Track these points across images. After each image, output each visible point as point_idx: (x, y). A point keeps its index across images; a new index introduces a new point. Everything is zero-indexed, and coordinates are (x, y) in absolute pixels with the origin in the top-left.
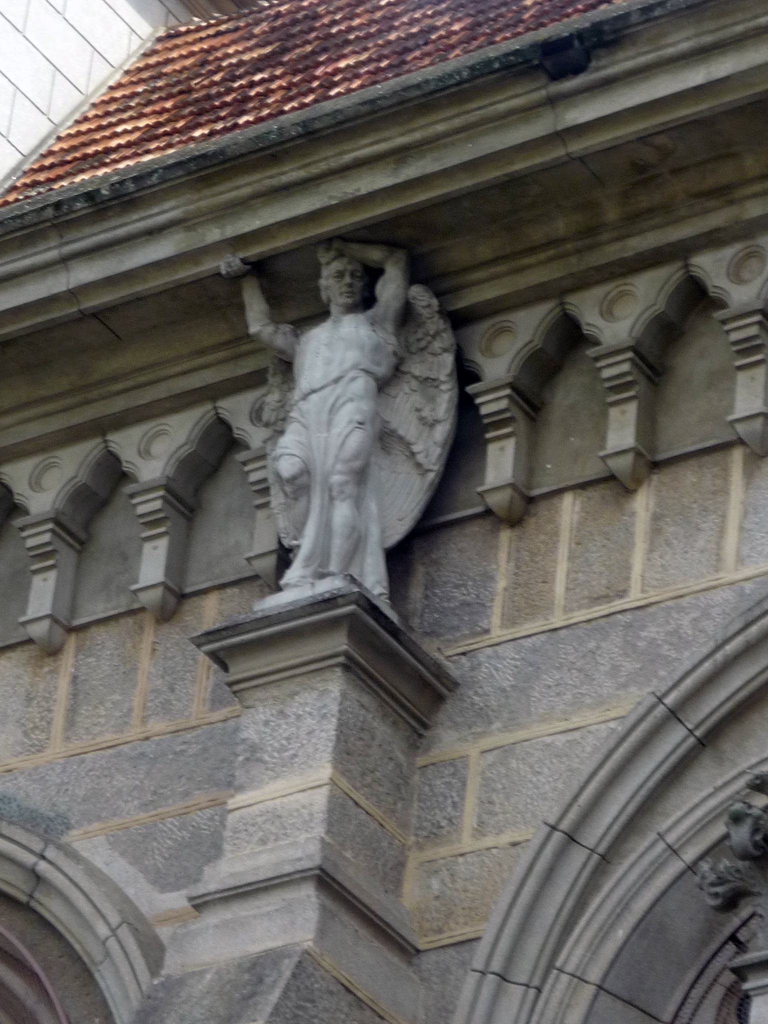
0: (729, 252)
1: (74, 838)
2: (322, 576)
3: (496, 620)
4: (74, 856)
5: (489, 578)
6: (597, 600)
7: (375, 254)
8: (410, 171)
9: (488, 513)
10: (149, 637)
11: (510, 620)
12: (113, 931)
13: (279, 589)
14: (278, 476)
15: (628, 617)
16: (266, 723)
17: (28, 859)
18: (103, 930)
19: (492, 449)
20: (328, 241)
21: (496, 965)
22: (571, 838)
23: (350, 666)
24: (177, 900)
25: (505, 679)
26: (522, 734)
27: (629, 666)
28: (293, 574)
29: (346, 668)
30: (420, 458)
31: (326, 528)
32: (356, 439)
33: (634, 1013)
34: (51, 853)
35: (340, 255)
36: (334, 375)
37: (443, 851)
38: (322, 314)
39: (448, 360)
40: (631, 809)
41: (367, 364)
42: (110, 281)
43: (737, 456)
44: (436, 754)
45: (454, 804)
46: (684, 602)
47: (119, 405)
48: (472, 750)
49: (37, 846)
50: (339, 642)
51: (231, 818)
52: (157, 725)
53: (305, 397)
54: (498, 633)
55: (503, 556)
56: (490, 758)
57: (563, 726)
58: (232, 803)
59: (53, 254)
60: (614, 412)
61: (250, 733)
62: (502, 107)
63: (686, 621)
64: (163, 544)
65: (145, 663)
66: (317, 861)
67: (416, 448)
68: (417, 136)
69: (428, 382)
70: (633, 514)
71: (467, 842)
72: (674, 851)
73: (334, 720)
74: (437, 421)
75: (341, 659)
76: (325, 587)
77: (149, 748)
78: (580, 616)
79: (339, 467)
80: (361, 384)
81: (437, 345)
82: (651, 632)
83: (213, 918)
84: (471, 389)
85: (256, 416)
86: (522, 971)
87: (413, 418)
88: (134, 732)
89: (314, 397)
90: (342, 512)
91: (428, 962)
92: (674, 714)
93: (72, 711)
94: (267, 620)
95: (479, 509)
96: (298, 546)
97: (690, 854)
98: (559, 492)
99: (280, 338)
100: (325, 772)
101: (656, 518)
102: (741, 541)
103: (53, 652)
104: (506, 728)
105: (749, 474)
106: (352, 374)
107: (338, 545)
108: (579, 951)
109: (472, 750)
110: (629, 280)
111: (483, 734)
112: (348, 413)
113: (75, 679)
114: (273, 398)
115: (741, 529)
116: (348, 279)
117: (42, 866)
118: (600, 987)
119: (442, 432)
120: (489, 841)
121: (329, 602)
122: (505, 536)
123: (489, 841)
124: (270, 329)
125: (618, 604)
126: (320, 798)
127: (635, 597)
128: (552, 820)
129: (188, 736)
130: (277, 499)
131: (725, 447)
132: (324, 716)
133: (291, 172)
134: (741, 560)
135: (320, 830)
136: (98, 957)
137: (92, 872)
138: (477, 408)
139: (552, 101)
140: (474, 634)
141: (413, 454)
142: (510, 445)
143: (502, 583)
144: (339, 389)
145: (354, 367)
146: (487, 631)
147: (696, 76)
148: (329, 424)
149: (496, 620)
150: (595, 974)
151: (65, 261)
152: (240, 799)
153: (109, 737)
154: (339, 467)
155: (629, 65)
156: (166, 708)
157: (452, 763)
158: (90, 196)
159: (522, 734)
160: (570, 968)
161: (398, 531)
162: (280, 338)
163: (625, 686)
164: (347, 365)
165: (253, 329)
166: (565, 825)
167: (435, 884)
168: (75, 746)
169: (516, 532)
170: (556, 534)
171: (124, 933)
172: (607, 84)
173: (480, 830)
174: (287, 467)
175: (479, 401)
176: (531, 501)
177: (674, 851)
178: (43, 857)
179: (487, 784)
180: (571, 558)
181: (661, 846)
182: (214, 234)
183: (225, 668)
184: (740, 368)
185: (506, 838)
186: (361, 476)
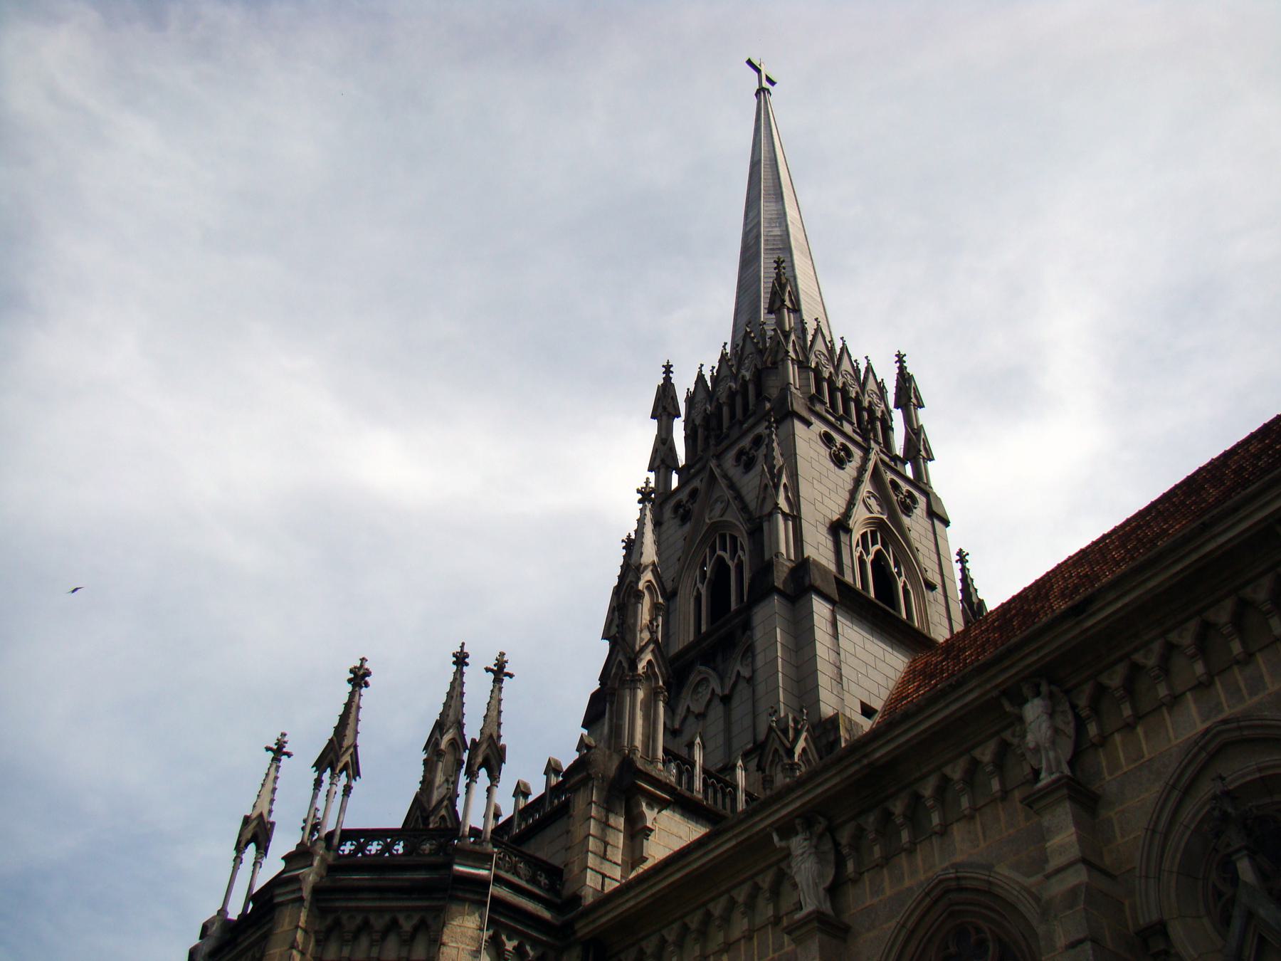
1: (997, 869)
2: (1052, 773)
3: (1106, 774)
4: (999, 874)
8: (1041, 654)
9: (1093, 745)
12: (1019, 892)
13: (1040, 781)
14: (1029, 749)
17: (986, 878)
18: (1016, 893)
19: (1089, 726)
21: (1143, 874)
22: (1154, 831)
23: (1070, 798)
24: (1038, 878)
28: (1043, 775)
31: (1048, 760)
34: (992, 874)
38: (1025, 701)
39: (1067, 704)
42: (962, 708)
43: (1164, 710)
49: (987, 873)
50: (1065, 791)
51: (1048, 850)
53: (1030, 724)
54: (1108, 778)
55: (1102, 754)
58: (1046, 846)
59: (943, 704)
60: (1122, 706)
61: (1046, 824)
64: (997, 779)
66: (1080, 855)
69: (1063, 712)
72: (1187, 827)
76: (1054, 777)
80: (1045, 717)
83: (1053, 880)
84: (1077, 711)
85: (1013, 735)
89: (1033, 724)
90: (1051, 754)
92: (1173, 787)
93: (984, 833)
94: (1040, 790)
96: (1042, 768)
97: (1192, 827)
98: (1113, 733)
100: (1073, 829)
101: (1146, 733)
105: (1170, 713)
107: (1053, 764)
112: (1044, 726)
114: (1018, 729)
117: (991, 879)
119: (1072, 725)
120: (1127, 839)
121: (1054, 782)
122: (1101, 750)
123: (1127, 839)
125: (1142, 761)
126: (1074, 838)
127: (1147, 756)
128: (1146, 827)
130: (1028, 755)
131: (1160, 707)
133: (1006, 663)
135: (1077, 847)
137: (1006, 877)
142: (1094, 723)
143: (1104, 764)
147: (1119, 604)
148: (1040, 731)
149: (1106, 774)
150: (1175, 869)
151: (947, 706)
152: (1048, 844)
158: (950, 686)
161: (1069, 757)
165: (1008, 710)
166: (1151, 827)
171: (1024, 893)
172: (1094, 614)
173: (1123, 836)
174: (1031, 745)
178: (990, 876)
182: (989, 686)
183: (1031, 807)
185: (1132, 836)
186: (1053, 743)
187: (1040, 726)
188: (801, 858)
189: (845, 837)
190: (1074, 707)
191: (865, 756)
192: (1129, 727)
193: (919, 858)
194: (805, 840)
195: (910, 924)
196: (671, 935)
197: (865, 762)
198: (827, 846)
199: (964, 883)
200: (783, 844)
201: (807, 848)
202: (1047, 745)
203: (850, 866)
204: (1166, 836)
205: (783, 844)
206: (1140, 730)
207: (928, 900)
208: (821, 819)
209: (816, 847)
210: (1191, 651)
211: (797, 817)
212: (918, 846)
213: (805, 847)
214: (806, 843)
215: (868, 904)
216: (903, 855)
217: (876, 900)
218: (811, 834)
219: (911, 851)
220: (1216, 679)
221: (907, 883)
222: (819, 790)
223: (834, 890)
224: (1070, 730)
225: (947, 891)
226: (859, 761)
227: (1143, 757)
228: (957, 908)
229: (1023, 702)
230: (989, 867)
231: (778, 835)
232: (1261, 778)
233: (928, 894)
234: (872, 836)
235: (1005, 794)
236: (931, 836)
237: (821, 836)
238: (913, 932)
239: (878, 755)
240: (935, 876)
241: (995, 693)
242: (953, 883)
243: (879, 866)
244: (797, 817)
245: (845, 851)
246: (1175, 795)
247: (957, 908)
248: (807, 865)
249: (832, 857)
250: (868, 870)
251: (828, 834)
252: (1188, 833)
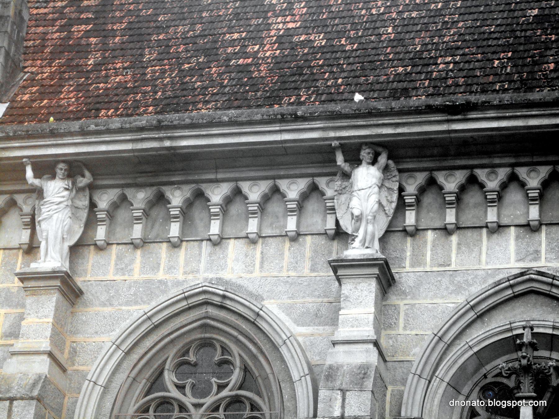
0: (487, 170)
5: (403, 251)
6: (441, 265)
7: (380, 149)
9: (404, 231)
10: (287, 244)
11: (412, 266)
15: (451, 273)
16: (351, 290)
20: (366, 144)
21: (418, 372)
22: (440, 339)
23: (378, 279)
25: (411, 283)
26: (417, 302)
27: (452, 288)
29: (377, 278)
30: (387, 212)
33: (455, 391)
35: (369, 148)
36: (369, 186)
37: (393, 332)
39: (398, 184)
40: (457, 332)
41: (378, 184)
44: (388, 302)
45: (396, 319)
46: (469, 272)
47: (282, 173)
48: (401, 303)
52: (292, 273)
54: (408, 269)
55: (409, 245)
56: (407, 307)
57: (431, 302)
59: (277, 128)
62: (433, 119)
63: (470, 278)
65: (287, 253)
67: (386, 209)
68: (404, 121)
70: (451, 241)
71: (401, 331)
72: (471, 348)
73: (374, 294)
74: (393, 202)
75: (376, 276)
77: (290, 280)
78: (435, 269)
79: (371, 214)
81: (394, 179)
82: (458, 279)
84: (403, 193)
86: (425, 375)
87: (385, 199)
88: (284, 274)
91: (388, 363)
93: (262, 263)
95: (401, 229)
97: (476, 349)
99: (346, 167)
101: (459, 244)
102: (487, 257)
103: (254, 242)
104: (412, 299)
105: (488, 237)
106: (374, 186)
107: (368, 238)
108: (443, 372)
109: (401, 303)
110: (454, 171)
111: (406, 299)
112: (374, 199)
113: (262, 253)
115: (487, 253)
116: (371, 155)
118: (448, 383)
122: (409, 239)
123: (408, 332)
124: (344, 164)
125: (447, 268)
127: (453, 267)
128: (435, 333)
129: (303, 279)
132: (371, 292)
134: (487, 263)
136: (281, 344)
138: (404, 200)
139: (448, 121)
140: (399, 267)
141: (385, 210)
143: (408, 254)
144: (371, 190)
145: (375, 184)
146: (405, 267)
150: (447, 379)
151: (281, 131)
153: (276, 274)
154: (371, 214)
155: (475, 116)
156: (295, 269)
157: (395, 306)
159: (417, 302)
160: (440, 376)
162: (346, 167)
163: (451, 293)
164: (373, 183)
165: (338, 163)
166: (439, 335)
167: (391, 342)
168: (263, 274)
169: (412, 239)
170: (426, 242)
173: (405, 328)
175: (405, 198)
176: (417, 230)
177: (471, 348)
178: (261, 310)
179: (406, 314)
180: (432, 250)
181: (467, 346)
184: (489, 206)
185: (414, 332)
187: (369, 196)
188: (56, 207)
191: (170, 138)
192: (446, 231)
193: (182, 253)
194: (66, 189)
195: (156, 320)
197: (167, 144)
199: (228, 303)
200: (37, 182)
201: (65, 199)
202: (370, 217)
204: (449, 346)
205: (37, 182)
206: (454, 239)
207: (184, 303)
209: (72, 200)
210: (534, 194)
211: (63, 161)
212: (184, 244)
213: (63, 197)
214: (66, 193)
215: (110, 277)
216: (165, 245)
217: (118, 278)
218: (74, 183)
219: (175, 246)
220: (544, 228)
221: (161, 275)
222: (103, 148)
225: (206, 303)
226: (161, 139)
227: (449, 265)
228: (208, 321)
229: (356, 161)
230: (259, 298)
231: (34, 170)
232: (553, 335)
233: (186, 298)
235: (296, 237)
236: (202, 240)
238: (156, 327)
239: (184, 143)
240: (200, 285)
241: (335, 143)
242: (217, 300)
243: (135, 246)
244: (63, 161)
246: (471, 315)
247: (208, 321)
248: (60, 216)
249: (84, 214)
250: (118, 244)
252: (470, 353)
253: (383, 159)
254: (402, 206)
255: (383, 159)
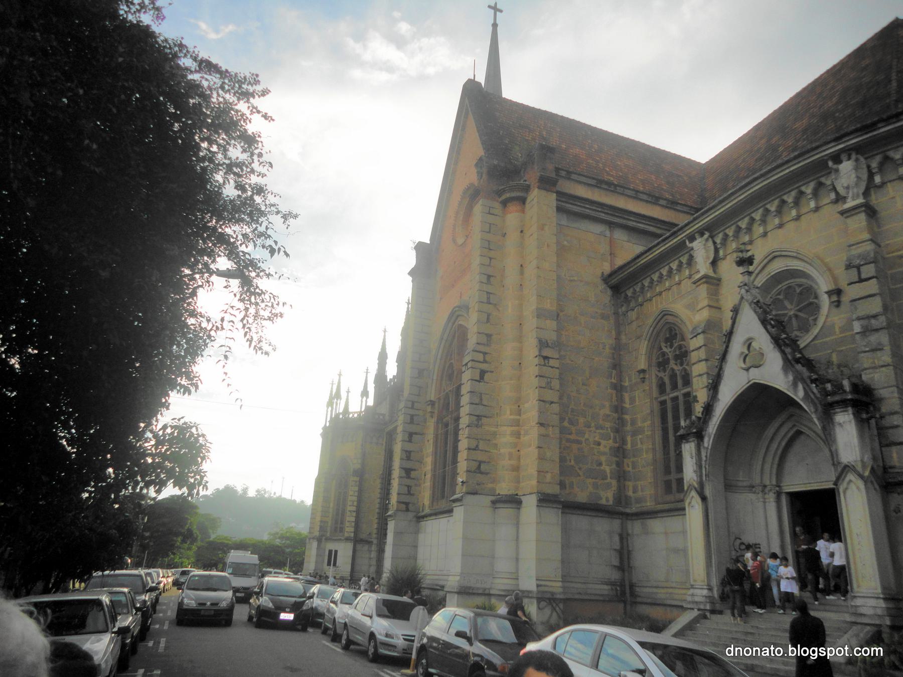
28: (848, 200)
31: (853, 192)
32: (855, 179)
112: (854, 176)
189: (718, 240)
190: (869, 167)
196: (674, 265)
198: (710, 243)
203: (721, 253)
208: (706, 233)
223: (714, 263)
224: (865, 176)
234: (732, 239)
237: (707, 240)
245: (719, 246)
251: (710, 239)
253: (854, 156)
254: (871, 175)
255: (854, 156)
